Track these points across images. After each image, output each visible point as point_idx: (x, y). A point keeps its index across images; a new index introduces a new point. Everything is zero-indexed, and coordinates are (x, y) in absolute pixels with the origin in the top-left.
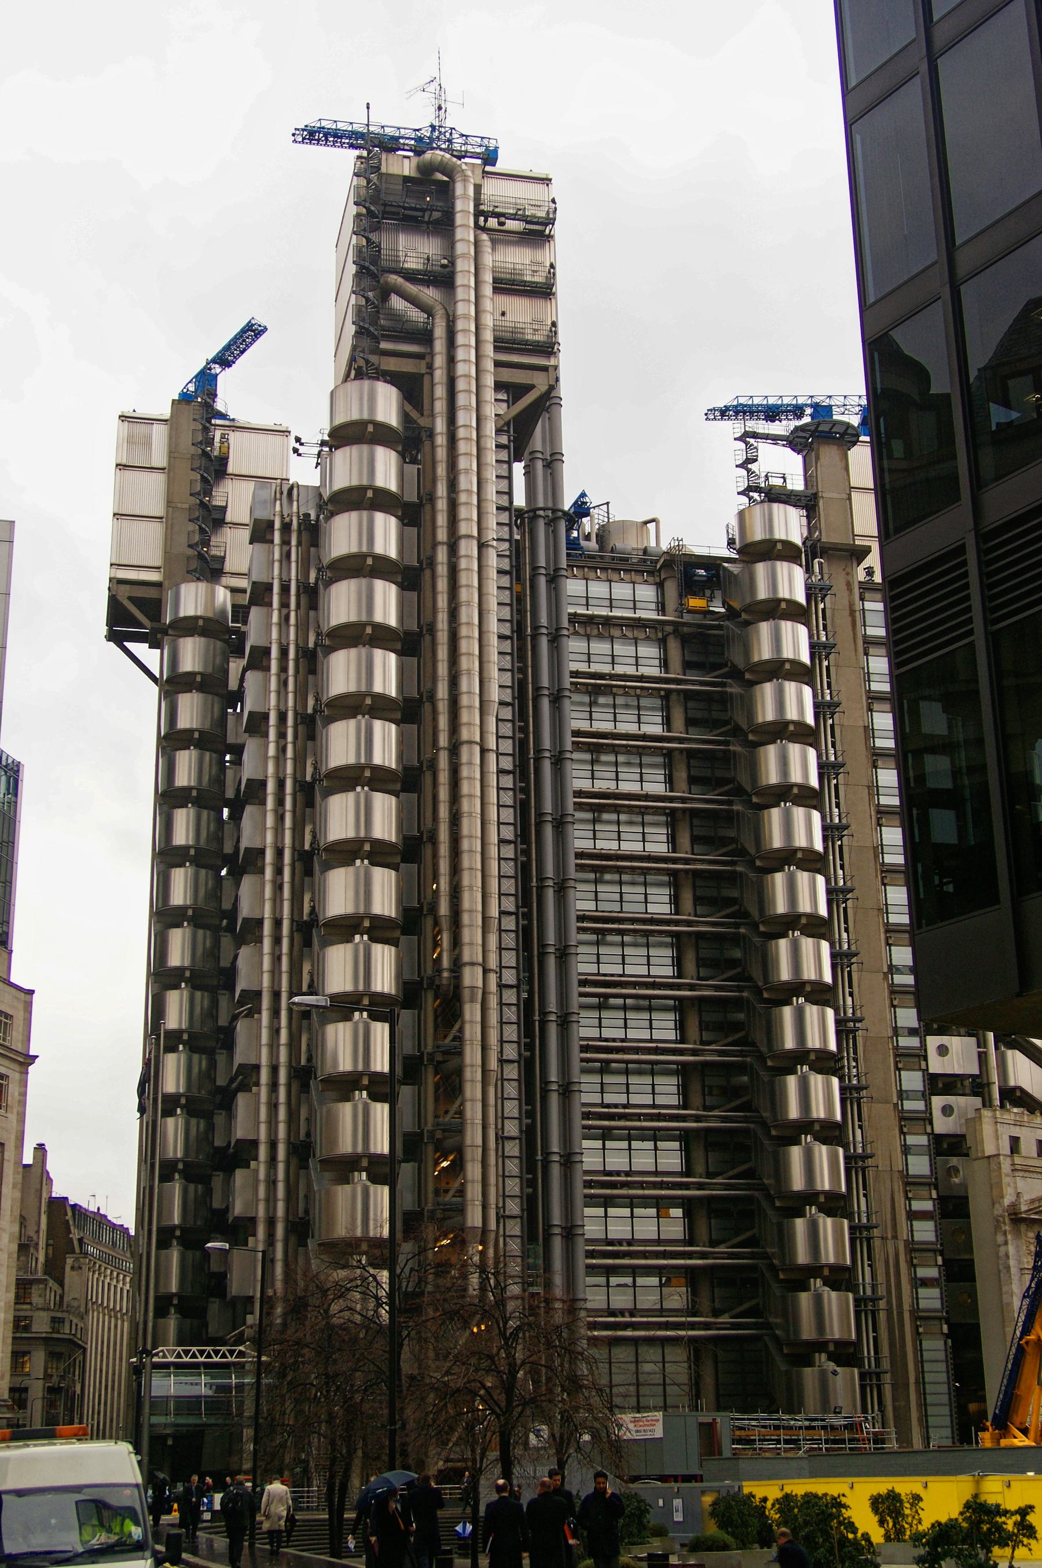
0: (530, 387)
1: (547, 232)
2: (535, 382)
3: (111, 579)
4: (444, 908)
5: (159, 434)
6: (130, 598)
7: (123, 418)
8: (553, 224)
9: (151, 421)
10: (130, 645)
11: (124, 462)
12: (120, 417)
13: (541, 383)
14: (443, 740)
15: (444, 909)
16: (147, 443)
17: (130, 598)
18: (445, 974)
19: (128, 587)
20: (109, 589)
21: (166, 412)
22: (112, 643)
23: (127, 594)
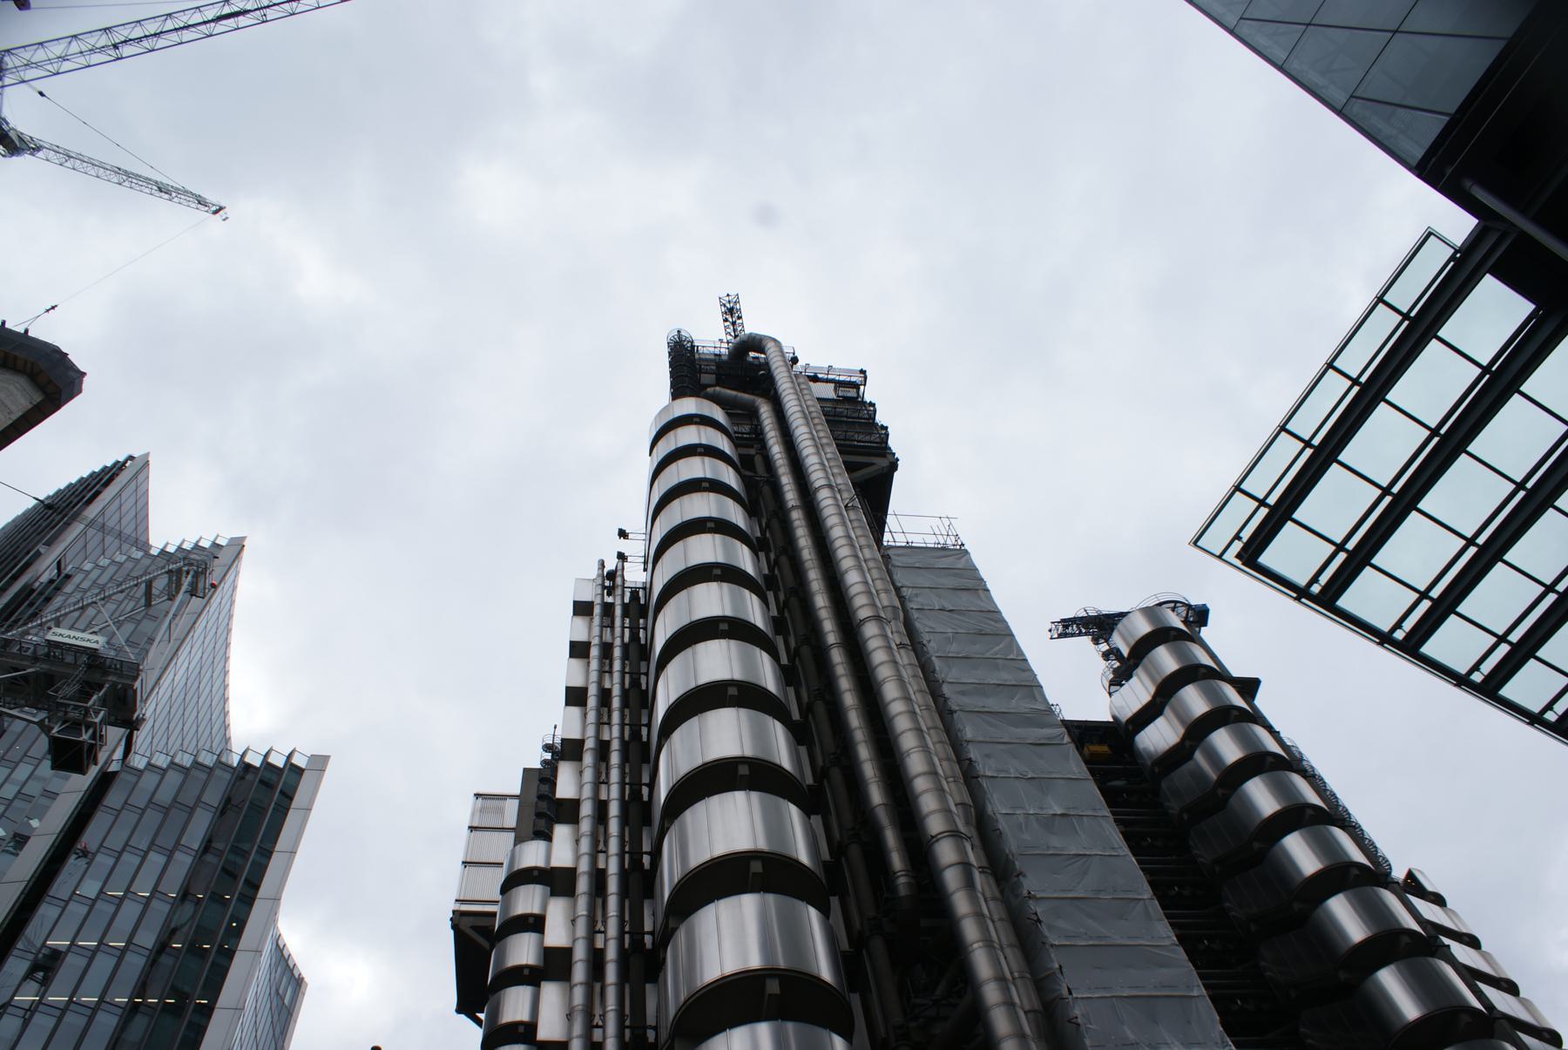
0: (873, 464)
1: (860, 399)
2: (874, 462)
3: (454, 912)
4: (876, 795)
5: (512, 808)
6: (473, 928)
7: (477, 796)
8: (865, 385)
9: (504, 797)
10: (479, 1015)
11: (475, 825)
12: (475, 795)
13: (882, 463)
14: (832, 637)
15: (876, 795)
16: (501, 811)
17: (473, 928)
18: (902, 880)
19: (471, 919)
20: (451, 919)
21: (516, 789)
22: (463, 1016)
23: (470, 924)
